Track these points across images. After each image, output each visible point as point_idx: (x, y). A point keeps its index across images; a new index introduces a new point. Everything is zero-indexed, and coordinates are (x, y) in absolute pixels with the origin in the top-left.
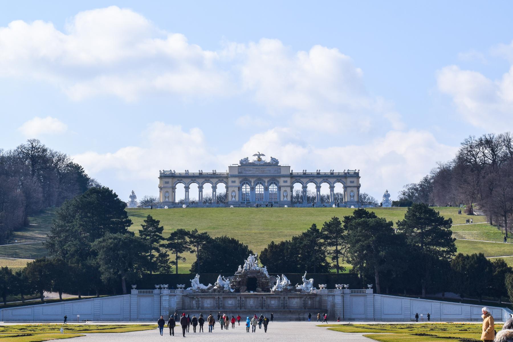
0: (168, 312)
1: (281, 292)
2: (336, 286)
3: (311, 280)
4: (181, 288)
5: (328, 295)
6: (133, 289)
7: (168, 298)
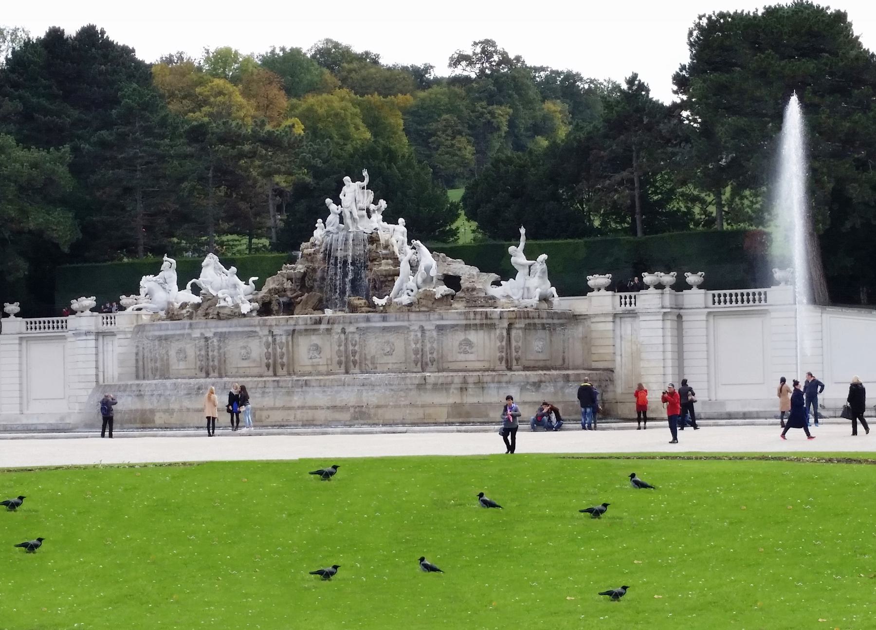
2: (648, 278)
5: (615, 315)
6: (7, 315)
7: (92, 343)
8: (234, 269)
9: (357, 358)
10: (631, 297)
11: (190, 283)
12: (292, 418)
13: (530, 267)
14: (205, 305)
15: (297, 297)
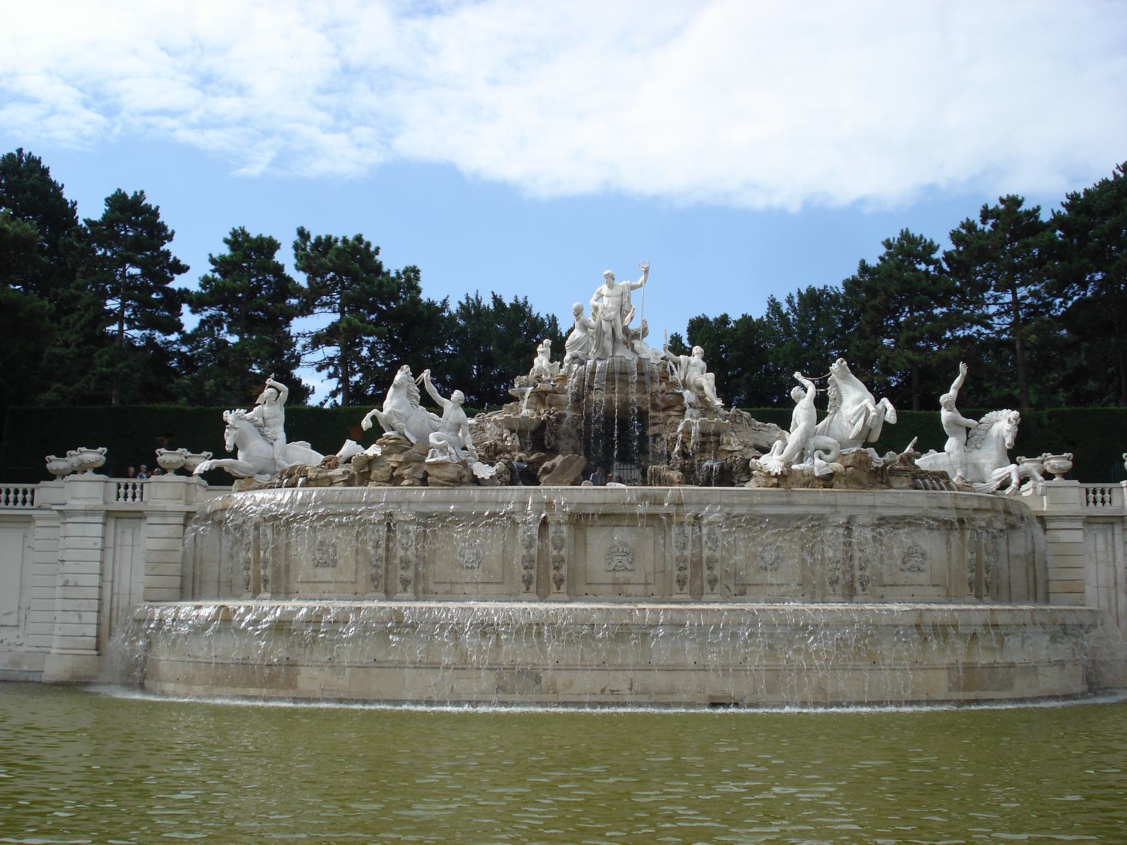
0: (93, 617)
1: (828, 480)
3: (1003, 423)
4: (184, 471)
5: (1090, 521)
8: (457, 394)
9: (717, 572)
10: (1103, 492)
11: (369, 415)
12: (624, 687)
13: (968, 429)
14: (393, 459)
15: (540, 461)
